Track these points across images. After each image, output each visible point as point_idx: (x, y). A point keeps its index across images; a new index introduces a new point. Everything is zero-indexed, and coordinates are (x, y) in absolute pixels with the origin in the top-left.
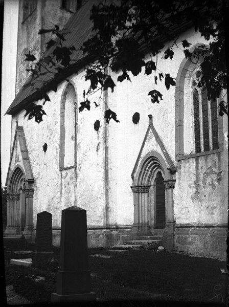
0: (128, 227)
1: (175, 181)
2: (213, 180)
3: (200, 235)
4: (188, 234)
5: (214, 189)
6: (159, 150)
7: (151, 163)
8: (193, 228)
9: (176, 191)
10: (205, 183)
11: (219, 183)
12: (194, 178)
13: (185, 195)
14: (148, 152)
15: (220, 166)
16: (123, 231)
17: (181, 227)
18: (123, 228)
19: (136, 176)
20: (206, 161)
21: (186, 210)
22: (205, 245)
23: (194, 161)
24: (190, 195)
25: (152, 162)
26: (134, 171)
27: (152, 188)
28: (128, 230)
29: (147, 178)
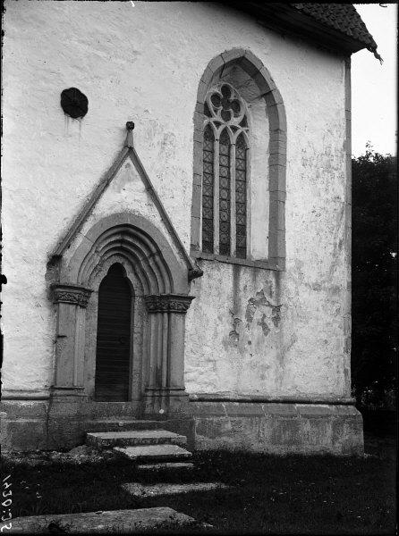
0: (25, 395)
2: (264, 316)
3: (249, 416)
4: (223, 415)
5: (266, 334)
6: (156, 220)
7: (113, 239)
8: (225, 403)
9: (191, 321)
10: (250, 319)
11: (276, 325)
12: (228, 304)
13: (209, 334)
14: (118, 209)
15: (278, 295)
17: (200, 400)
19: (74, 258)
20: (254, 280)
21: (211, 365)
22: (259, 436)
23: (231, 271)
24: (221, 337)
25: (118, 237)
26: (66, 241)
27: (94, 298)
28: (24, 403)
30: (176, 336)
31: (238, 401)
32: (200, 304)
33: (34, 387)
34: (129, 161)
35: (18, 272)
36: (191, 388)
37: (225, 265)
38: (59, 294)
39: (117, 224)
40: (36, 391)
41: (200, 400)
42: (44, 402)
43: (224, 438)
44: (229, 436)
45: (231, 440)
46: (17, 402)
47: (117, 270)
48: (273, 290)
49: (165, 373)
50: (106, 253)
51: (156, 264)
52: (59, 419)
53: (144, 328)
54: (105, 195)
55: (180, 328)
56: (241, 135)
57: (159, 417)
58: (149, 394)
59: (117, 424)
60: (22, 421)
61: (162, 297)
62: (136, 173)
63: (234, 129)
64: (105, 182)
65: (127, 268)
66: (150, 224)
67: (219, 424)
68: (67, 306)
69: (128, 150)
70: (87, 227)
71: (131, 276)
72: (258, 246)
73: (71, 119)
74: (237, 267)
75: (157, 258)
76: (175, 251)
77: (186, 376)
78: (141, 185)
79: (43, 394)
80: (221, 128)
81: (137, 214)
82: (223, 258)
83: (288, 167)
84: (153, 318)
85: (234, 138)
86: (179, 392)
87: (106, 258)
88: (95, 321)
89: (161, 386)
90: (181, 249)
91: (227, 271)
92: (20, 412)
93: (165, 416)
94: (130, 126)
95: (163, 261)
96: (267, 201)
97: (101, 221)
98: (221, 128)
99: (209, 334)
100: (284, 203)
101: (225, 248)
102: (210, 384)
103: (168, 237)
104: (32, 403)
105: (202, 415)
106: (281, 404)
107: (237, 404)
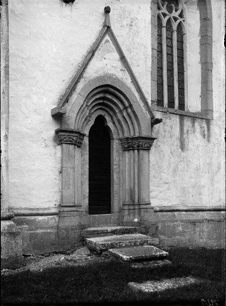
0: (40, 212)
4: (177, 221)
6: (128, 81)
7: (98, 96)
14: (101, 73)
16: (28, 222)
17: (161, 211)
18: (24, 215)
21: (166, 186)
23: (178, 120)
26: (65, 99)
27: (86, 141)
28: (40, 218)
30: (145, 167)
31: (186, 211)
32: (159, 143)
33: (46, 206)
34: (107, 37)
35: (31, 121)
36: (155, 203)
37: (175, 115)
38: (65, 136)
39: (101, 84)
40: (48, 209)
41: (161, 211)
42: (54, 216)
43: (178, 237)
44: (181, 235)
45: (182, 238)
46: (36, 217)
47: (100, 120)
48: (206, 133)
49: (137, 193)
50: (93, 107)
51: (128, 114)
52: (66, 229)
53: (121, 161)
54: (92, 63)
55: (146, 160)
56: (180, 24)
57: (133, 223)
58: (126, 207)
59: (107, 231)
60: (39, 231)
61: (133, 139)
62: (113, 47)
63: (175, 19)
64: (92, 53)
65: (108, 118)
66: (124, 84)
67: (174, 227)
68: (68, 145)
69: (107, 29)
70: (80, 86)
71: (110, 125)
72: (193, 103)
73: (64, 4)
74: (182, 117)
75: (129, 110)
76: (142, 104)
77: (152, 195)
78: (116, 56)
79: (54, 211)
80: (167, 18)
81: (114, 77)
82: (171, 110)
83: (213, 45)
84: (127, 152)
85: (175, 26)
86: (148, 206)
87: (93, 111)
88: (87, 157)
89: (134, 201)
90: (146, 103)
91: (176, 119)
92: (38, 226)
93: (139, 223)
94: (107, 10)
95: (134, 112)
96: (200, 70)
97: (89, 82)
98: (167, 18)
99: (165, 164)
100: (211, 71)
101: (171, 104)
102: (166, 199)
103: (137, 95)
104: (45, 218)
105: (163, 222)
106: (212, 212)
107: (184, 213)
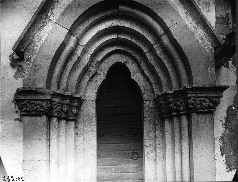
1: (223, 89)
27: (90, 109)
29: (78, 73)
47: (118, 72)
65: (131, 66)
71: (137, 77)
84: (167, 123)
87: (99, 58)
